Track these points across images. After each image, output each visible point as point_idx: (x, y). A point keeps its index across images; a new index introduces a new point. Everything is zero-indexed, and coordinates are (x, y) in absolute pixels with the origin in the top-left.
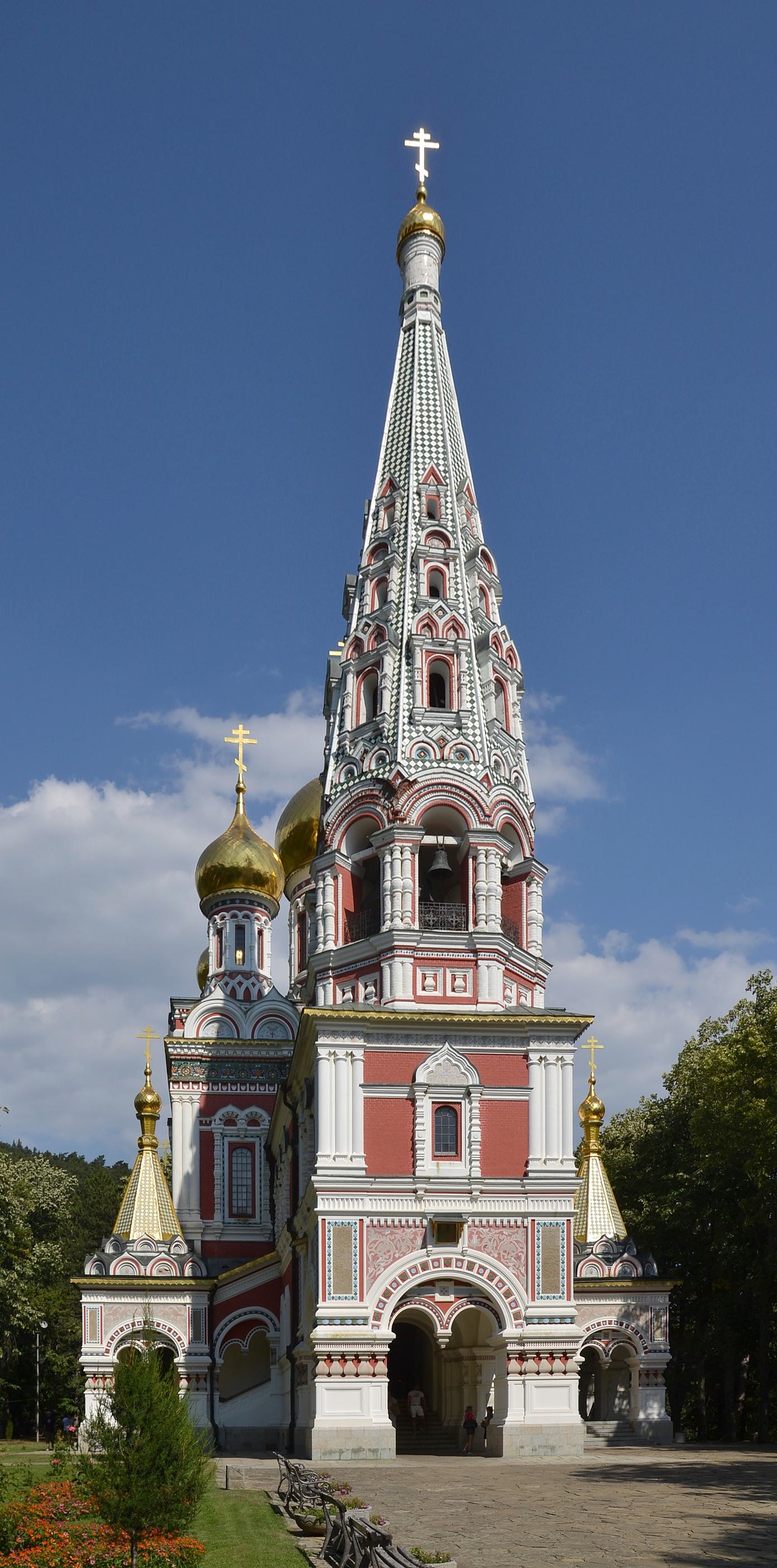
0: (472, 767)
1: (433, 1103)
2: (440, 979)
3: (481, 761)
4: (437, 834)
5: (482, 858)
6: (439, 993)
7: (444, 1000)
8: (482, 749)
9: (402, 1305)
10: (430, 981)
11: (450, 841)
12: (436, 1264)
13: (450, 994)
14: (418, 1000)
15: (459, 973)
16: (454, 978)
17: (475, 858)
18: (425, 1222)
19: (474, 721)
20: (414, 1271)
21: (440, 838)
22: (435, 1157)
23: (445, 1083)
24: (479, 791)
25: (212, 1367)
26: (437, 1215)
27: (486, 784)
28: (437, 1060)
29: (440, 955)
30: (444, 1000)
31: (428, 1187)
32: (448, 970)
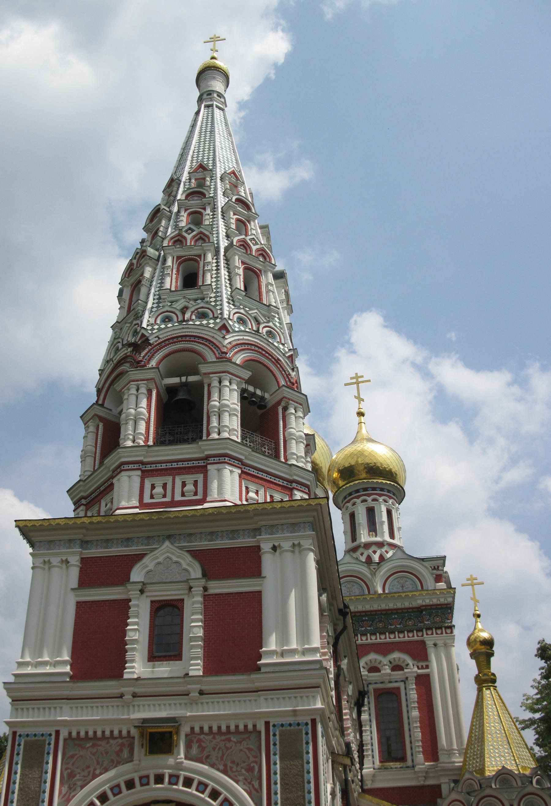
0: (212, 321)
1: (152, 602)
3: (220, 316)
4: (180, 376)
5: (215, 383)
6: (168, 499)
7: (174, 503)
10: (159, 490)
11: (191, 379)
13: (178, 497)
14: (148, 506)
15: (189, 479)
16: (184, 484)
17: (209, 385)
18: (134, 732)
20: (116, 790)
21: (184, 379)
23: (164, 581)
24: (216, 336)
26: (145, 721)
27: (224, 332)
28: (157, 558)
29: (169, 466)
31: (137, 690)
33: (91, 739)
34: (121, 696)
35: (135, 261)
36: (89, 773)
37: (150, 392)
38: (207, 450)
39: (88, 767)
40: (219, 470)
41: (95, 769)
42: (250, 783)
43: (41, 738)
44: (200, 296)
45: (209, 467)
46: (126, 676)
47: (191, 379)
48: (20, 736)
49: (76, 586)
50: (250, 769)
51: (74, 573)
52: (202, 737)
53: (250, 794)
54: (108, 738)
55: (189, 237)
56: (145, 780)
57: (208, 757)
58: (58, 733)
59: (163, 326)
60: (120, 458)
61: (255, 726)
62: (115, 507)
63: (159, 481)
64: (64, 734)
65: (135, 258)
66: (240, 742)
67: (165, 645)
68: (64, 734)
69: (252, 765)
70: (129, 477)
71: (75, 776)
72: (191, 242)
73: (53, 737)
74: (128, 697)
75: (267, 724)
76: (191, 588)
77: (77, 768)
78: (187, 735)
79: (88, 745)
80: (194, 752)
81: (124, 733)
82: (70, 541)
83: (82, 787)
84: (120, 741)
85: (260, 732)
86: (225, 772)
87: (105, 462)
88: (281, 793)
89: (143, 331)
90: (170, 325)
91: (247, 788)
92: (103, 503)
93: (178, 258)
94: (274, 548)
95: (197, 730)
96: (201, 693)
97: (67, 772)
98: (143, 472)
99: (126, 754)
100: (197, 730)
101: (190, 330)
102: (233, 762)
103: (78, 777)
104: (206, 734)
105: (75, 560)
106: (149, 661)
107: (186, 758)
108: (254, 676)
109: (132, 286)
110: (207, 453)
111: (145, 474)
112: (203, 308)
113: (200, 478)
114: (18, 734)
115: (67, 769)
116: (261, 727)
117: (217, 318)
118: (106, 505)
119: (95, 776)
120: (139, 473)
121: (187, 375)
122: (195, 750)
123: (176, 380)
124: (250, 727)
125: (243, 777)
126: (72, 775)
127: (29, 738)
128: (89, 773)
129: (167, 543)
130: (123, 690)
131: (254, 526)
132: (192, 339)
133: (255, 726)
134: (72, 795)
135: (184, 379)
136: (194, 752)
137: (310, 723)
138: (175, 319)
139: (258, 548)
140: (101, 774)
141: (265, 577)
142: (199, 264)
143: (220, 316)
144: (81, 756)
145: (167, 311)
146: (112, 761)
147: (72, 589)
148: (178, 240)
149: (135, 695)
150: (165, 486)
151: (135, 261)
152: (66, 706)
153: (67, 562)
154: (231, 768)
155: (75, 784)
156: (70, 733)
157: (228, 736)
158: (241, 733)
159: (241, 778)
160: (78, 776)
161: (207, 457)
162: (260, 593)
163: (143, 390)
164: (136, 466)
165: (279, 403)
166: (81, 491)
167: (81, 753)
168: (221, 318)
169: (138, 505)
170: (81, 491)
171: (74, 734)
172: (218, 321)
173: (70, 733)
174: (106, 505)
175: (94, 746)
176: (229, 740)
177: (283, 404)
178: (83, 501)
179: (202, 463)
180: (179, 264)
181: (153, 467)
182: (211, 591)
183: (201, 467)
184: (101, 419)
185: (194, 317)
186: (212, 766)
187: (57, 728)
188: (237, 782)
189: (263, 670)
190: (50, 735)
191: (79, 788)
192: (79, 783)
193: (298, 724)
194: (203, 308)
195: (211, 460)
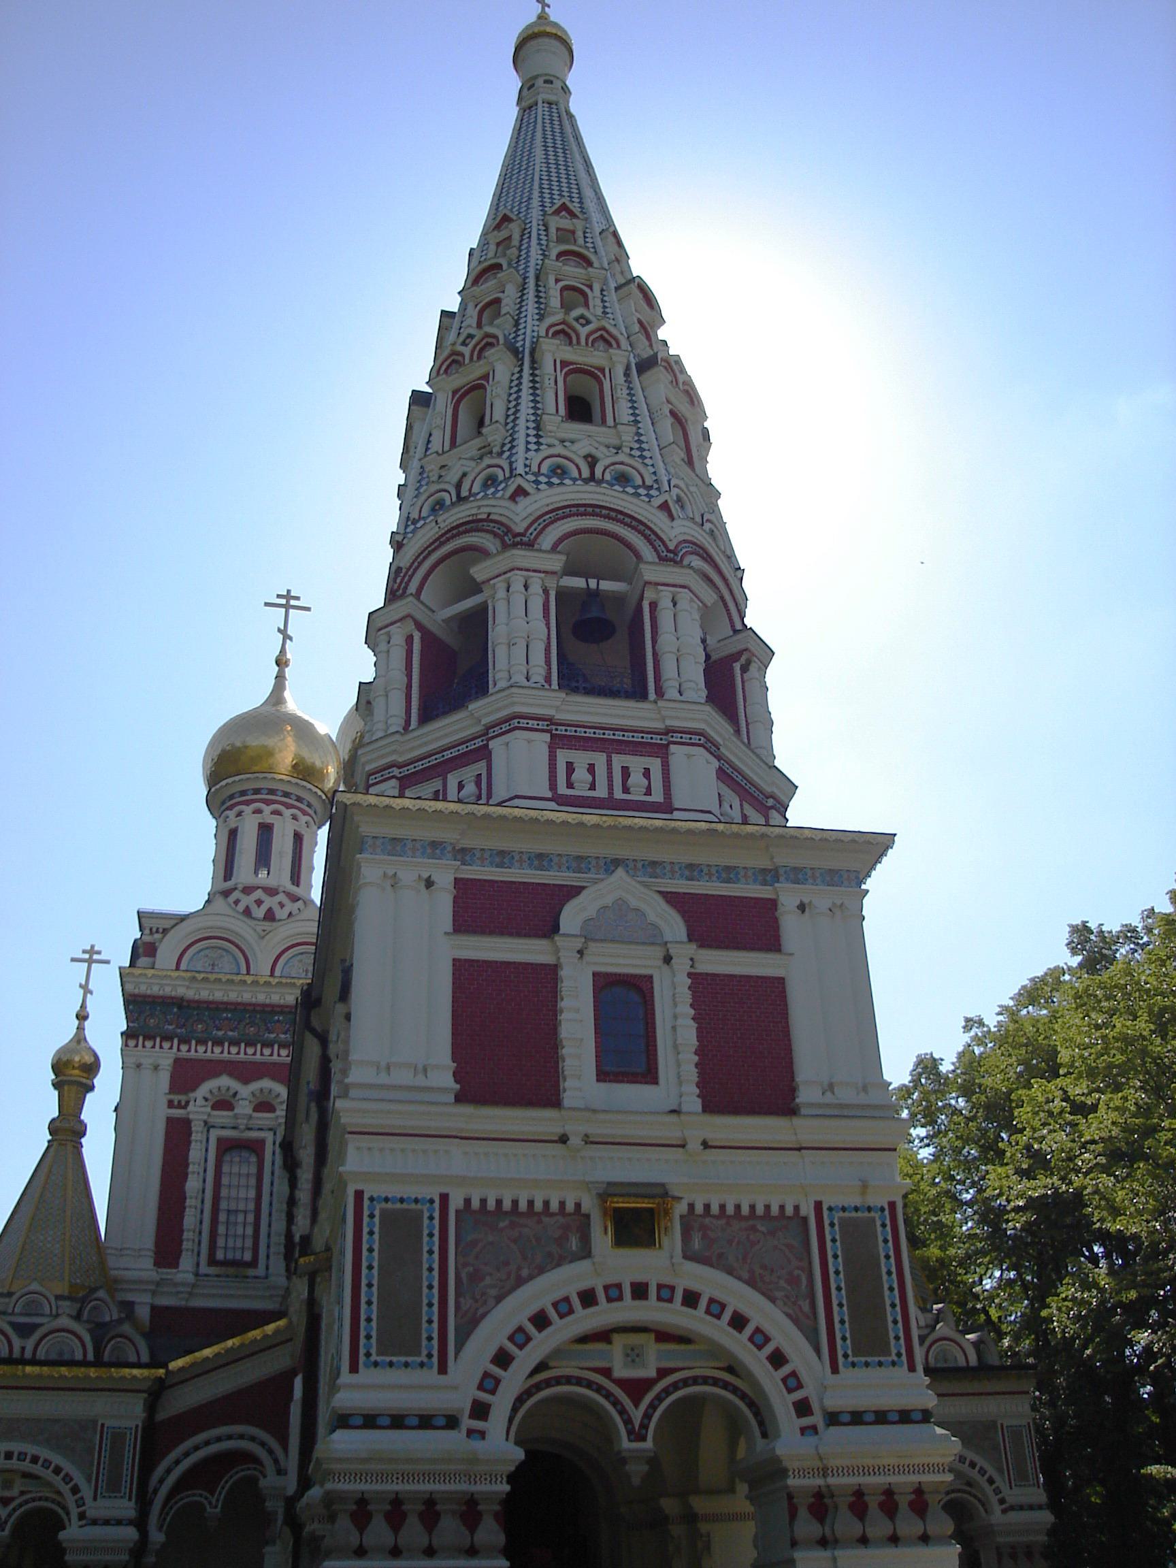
2: (601, 771)
3: (656, 486)
5: (665, 603)
8: (654, 473)
9: (538, 1387)
12: (614, 1293)
13: (619, 794)
15: (636, 763)
16: (626, 772)
17: (653, 606)
18: (589, 1204)
19: (639, 441)
21: (593, 583)
22: (603, 1076)
25: (140, 1549)
26: (609, 1184)
29: (599, 734)
30: (609, 803)
32: (615, 758)
33: (506, 1212)
34: (563, 1139)
35: (467, 351)
36: (509, 1274)
37: (546, 592)
38: (671, 718)
39: (507, 1264)
40: (689, 756)
41: (519, 1268)
42: (794, 1303)
43: (413, 1206)
44: (616, 442)
45: (673, 748)
46: (567, 1102)
47: (606, 585)
48: (372, 1199)
49: (449, 928)
50: (793, 1281)
51: (444, 903)
52: (707, 1220)
53: (796, 1322)
54: (538, 1214)
55: (583, 332)
56: (614, 1292)
57: (720, 1256)
58: (444, 1198)
59: (555, 480)
60: (513, 704)
61: (797, 1208)
62: (500, 792)
63: (582, 759)
64: (456, 1203)
65: (464, 344)
66: (772, 1233)
67: (628, 1053)
68: (456, 1203)
69: (796, 1272)
70: (529, 741)
71: (482, 1279)
72: (587, 340)
73: (437, 1205)
74: (575, 1141)
75: (818, 1206)
76: (668, 959)
77: (486, 1264)
78: (681, 1217)
79: (502, 1225)
80: (697, 1246)
81: (570, 1207)
82: (434, 844)
83: (499, 1299)
84: (561, 1220)
85: (805, 1220)
86: (751, 1283)
87: (472, 707)
88: (850, 1324)
89: (519, 481)
90: (567, 481)
91: (791, 1312)
92: (452, 780)
93: (564, 364)
94: (802, 907)
95: (699, 1209)
96: (706, 1145)
97: (466, 1270)
98: (553, 736)
99: (574, 1243)
100: (699, 1209)
101: (608, 499)
102: (764, 1267)
103: (488, 1281)
104: (714, 1216)
105: (445, 878)
106: (598, 1080)
107: (686, 1257)
108: (796, 1121)
109: (454, 393)
110: (669, 723)
111: (558, 742)
112: (622, 463)
113: (655, 764)
114: (366, 1196)
115: (465, 1265)
116: (808, 1210)
117: (651, 487)
118: (461, 786)
119: (520, 1282)
120: (547, 737)
121: (599, 578)
122: (696, 1244)
123: (578, 583)
124: (789, 1211)
125: (782, 1294)
126: (476, 1277)
127: (389, 1205)
128: (509, 1274)
129: (620, 872)
130: (568, 1129)
131: (765, 863)
132: (613, 514)
133: (797, 1208)
134: (481, 1311)
135: (593, 583)
136: (697, 1246)
137: (886, 1207)
138: (575, 474)
139: (773, 904)
140: (531, 1277)
141: (791, 954)
142: (601, 384)
143: (656, 486)
144: (492, 1243)
145: (559, 456)
146: (550, 1255)
147: (446, 933)
148: (562, 331)
149: (588, 1140)
150: (591, 769)
151: (467, 351)
152: (456, 1148)
153: (429, 883)
154: (761, 1276)
155: (483, 1294)
156: (468, 1201)
157: (751, 1222)
158: (776, 1218)
159: (779, 1294)
160: (488, 1278)
161: (668, 731)
162: (781, 981)
163: (536, 588)
164: (543, 725)
165: (736, 656)
166: (394, 752)
167: (490, 1239)
168: (658, 489)
169: (549, 795)
170: (394, 752)
171: (476, 1204)
172: (653, 492)
173: (468, 1201)
174: (461, 786)
175: (513, 1225)
176: (753, 1228)
177: (743, 659)
178: (396, 771)
179: (657, 740)
180: (566, 375)
181: (571, 732)
182: (702, 968)
183: (657, 746)
184: (419, 626)
185: (608, 477)
186: (730, 1272)
187: (445, 1191)
188: (773, 1300)
189: (803, 1111)
190: (432, 1201)
191: (491, 1302)
192: (493, 1292)
193: (869, 1209)
194: (622, 463)
195: (677, 737)
